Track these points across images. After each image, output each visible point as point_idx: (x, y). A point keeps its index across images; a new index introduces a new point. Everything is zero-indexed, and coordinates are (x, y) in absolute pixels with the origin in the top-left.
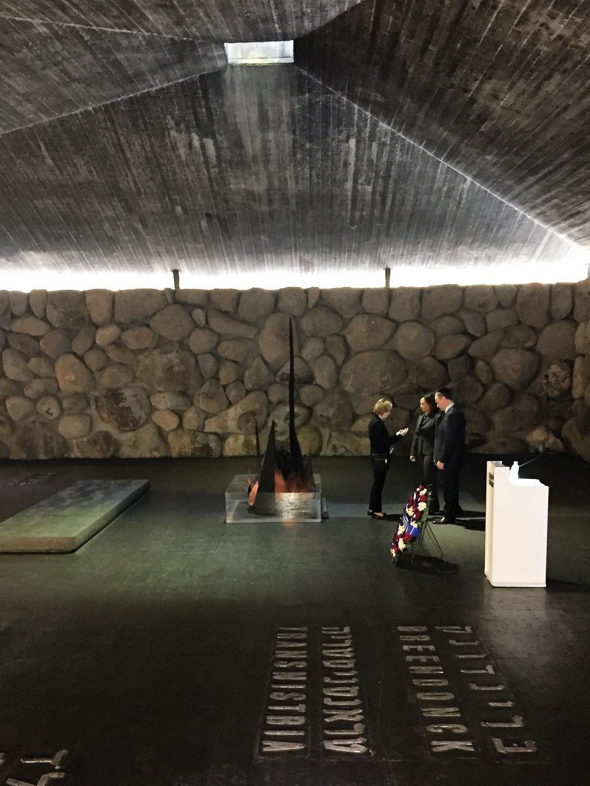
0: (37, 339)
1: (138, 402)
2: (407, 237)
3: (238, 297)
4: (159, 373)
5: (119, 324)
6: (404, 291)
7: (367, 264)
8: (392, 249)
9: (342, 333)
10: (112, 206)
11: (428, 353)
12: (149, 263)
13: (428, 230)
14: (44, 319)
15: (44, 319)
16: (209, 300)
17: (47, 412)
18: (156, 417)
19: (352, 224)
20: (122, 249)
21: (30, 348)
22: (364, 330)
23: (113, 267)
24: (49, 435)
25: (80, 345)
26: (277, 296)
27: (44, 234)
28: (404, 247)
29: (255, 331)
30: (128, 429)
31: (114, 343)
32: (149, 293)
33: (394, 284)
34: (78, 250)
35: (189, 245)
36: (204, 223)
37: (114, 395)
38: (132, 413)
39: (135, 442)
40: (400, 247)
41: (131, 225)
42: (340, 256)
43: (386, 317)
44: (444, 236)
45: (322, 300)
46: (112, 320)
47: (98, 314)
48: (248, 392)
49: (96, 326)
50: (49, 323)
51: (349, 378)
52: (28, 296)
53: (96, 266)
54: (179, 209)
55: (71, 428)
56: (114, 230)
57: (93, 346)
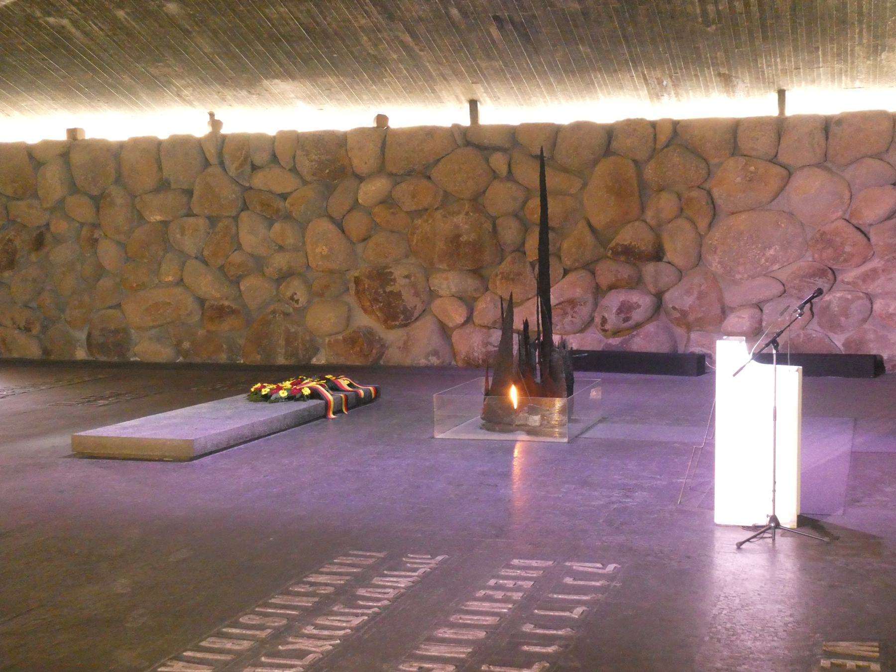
0: (284, 197)
1: (413, 285)
2: (795, 40)
3: (554, 133)
4: (441, 245)
5: (391, 175)
6: (801, 120)
7: (747, 80)
8: (778, 60)
9: (707, 186)
10: (366, 12)
11: (840, 213)
12: (434, 91)
13: (824, 31)
14: (294, 170)
15: (294, 170)
16: (513, 139)
17: (292, 298)
18: (436, 305)
19: (707, 23)
20: (393, 71)
21: (272, 209)
22: (739, 179)
23: (387, 98)
24: (293, 330)
25: (338, 203)
26: (610, 133)
27: (288, 55)
28: (796, 56)
29: (577, 184)
30: (397, 323)
31: (382, 202)
32: (429, 133)
33: (789, 112)
34: (336, 75)
35: (483, 65)
36: (495, 32)
37: (382, 276)
38: (403, 301)
39: (405, 343)
40: (790, 56)
41: (397, 37)
42: (702, 71)
43: (773, 160)
44: (853, 38)
45: (677, 137)
46: (381, 170)
47: (362, 161)
48: (566, 272)
49: (360, 179)
50: (301, 178)
51: (715, 252)
52: (273, 140)
53: (365, 97)
54: (454, 12)
55: (324, 320)
56: (375, 45)
57: (355, 205)
